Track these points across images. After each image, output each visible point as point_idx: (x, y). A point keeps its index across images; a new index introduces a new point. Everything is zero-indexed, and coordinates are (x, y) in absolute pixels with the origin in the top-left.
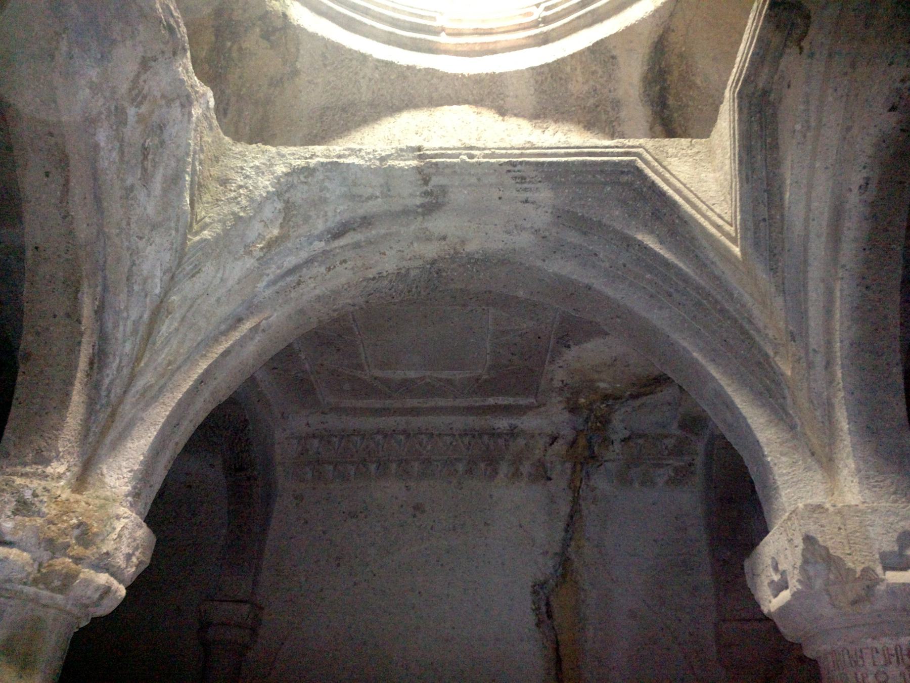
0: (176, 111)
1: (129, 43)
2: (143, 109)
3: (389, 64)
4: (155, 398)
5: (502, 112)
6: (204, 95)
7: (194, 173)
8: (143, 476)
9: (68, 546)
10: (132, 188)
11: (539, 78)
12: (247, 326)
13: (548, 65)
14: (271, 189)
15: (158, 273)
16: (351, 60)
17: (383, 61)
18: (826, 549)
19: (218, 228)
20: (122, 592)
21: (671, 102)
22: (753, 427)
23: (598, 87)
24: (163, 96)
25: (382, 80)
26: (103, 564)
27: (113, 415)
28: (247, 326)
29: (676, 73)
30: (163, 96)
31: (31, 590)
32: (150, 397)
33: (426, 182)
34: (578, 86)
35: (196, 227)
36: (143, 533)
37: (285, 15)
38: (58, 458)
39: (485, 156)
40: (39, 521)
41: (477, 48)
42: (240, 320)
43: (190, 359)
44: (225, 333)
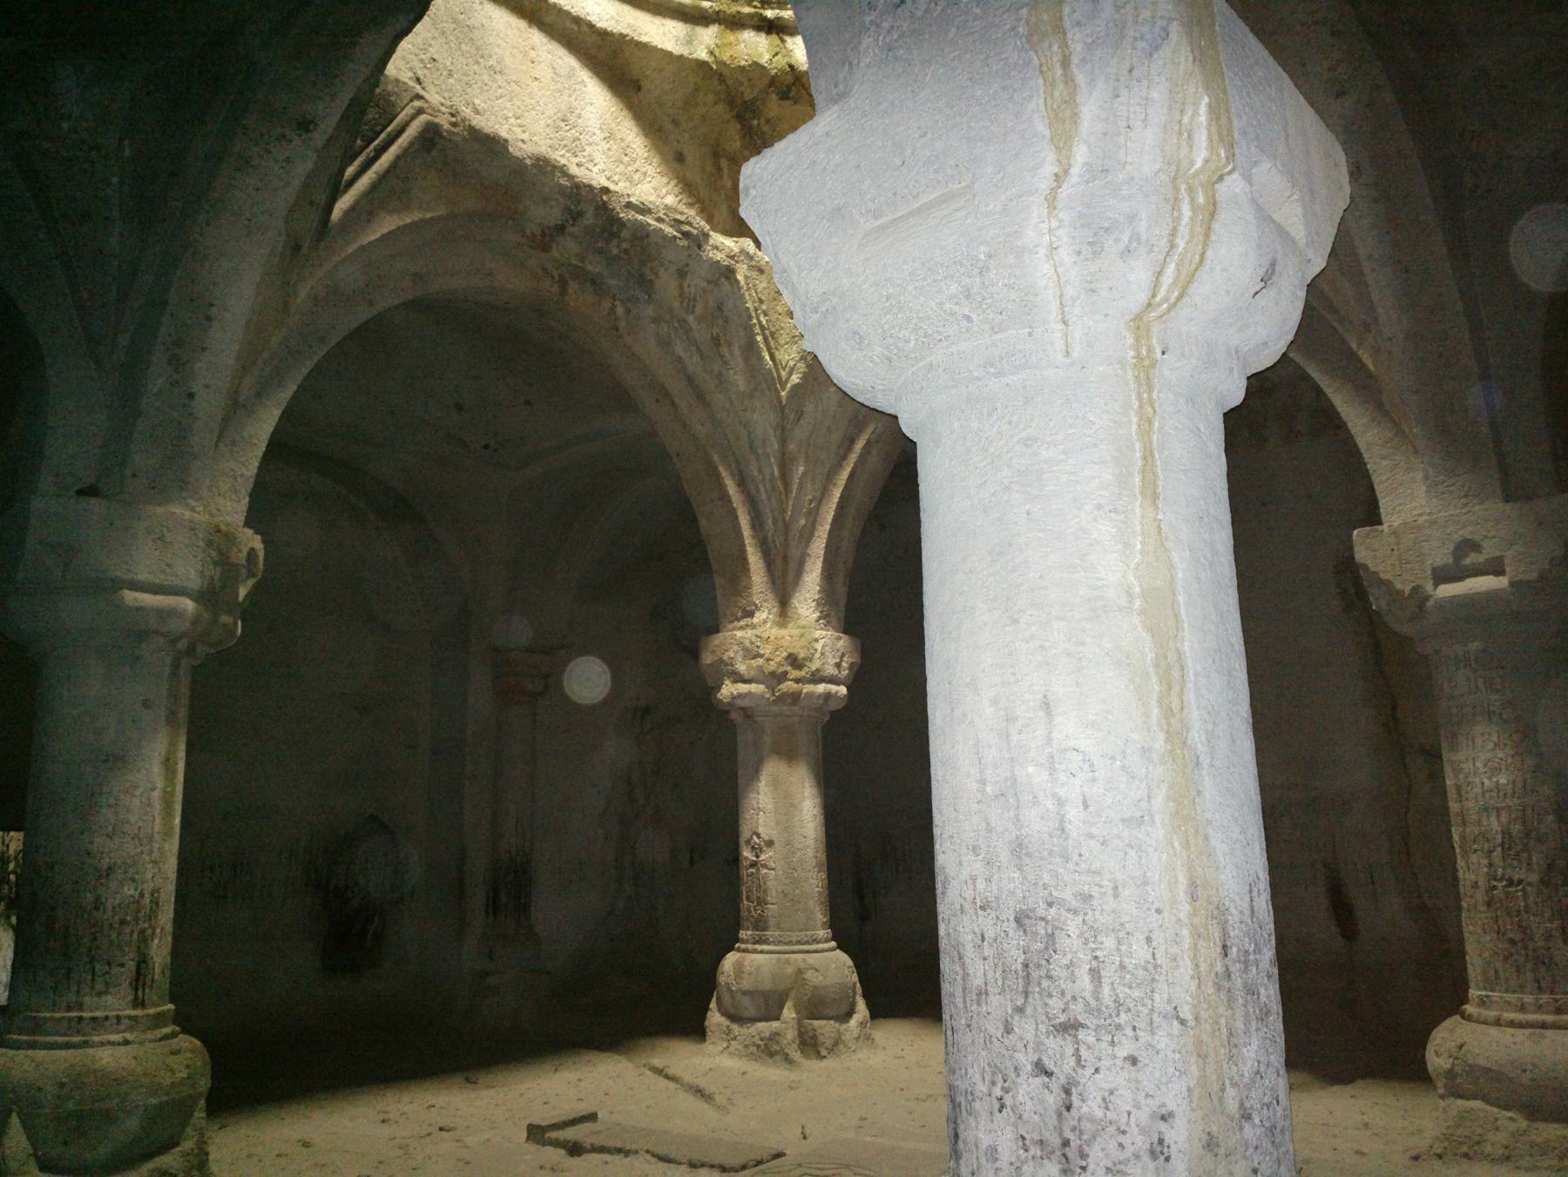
0: (726, 286)
1: (662, 271)
2: (699, 308)
4: (811, 535)
6: (742, 251)
7: (762, 328)
8: (827, 599)
9: (786, 673)
10: (720, 374)
12: (859, 445)
15: (771, 431)
19: (802, 367)
20: (843, 690)
22: (1353, 431)
24: (709, 282)
26: (816, 678)
27: (785, 559)
28: (859, 445)
30: (709, 282)
31: (775, 708)
32: (808, 535)
35: (783, 374)
36: (844, 642)
37: (791, 67)
38: (757, 608)
40: (760, 661)
42: (852, 441)
43: (824, 492)
44: (844, 457)
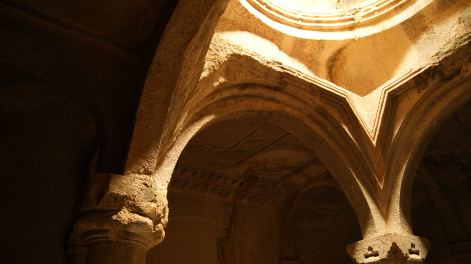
3: (246, 10)
5: (280, 48)
11: (296, 42)
13: (302, 39)
14: (226, 60)
16: (234, 2)
17: (245, 8)
18: (398, 247)
21: (333, 70)
23: (313, 54)
25: (241, 15)
29: (340, 62)
33: (281, 78)
34: (307, 50)
39: (304, 77)
41: (276, 18)
